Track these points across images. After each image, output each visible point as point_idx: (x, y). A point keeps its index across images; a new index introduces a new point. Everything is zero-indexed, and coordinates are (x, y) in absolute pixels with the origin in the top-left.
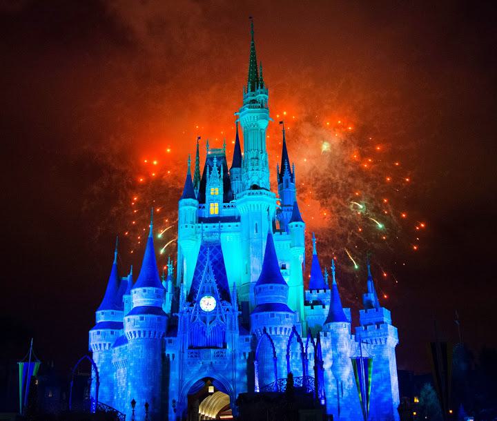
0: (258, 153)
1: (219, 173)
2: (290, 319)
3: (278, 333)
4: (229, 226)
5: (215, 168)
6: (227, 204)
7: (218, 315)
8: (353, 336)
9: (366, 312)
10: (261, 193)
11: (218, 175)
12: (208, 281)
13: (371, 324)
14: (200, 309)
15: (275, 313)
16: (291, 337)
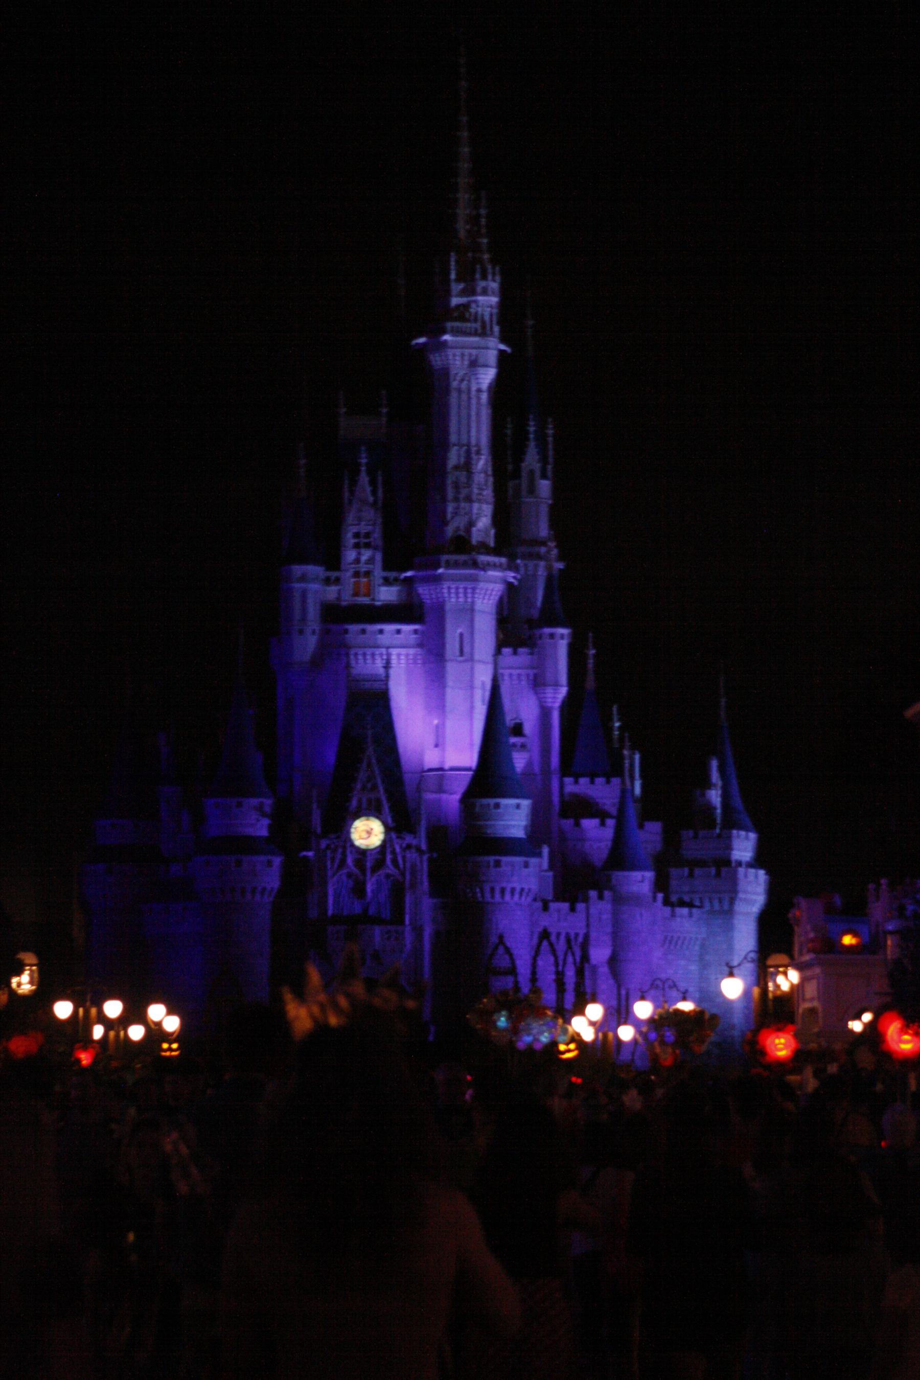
0: (468, 452)
1: (374, 492)
2: (531, 869)
3: (508, 897)
4: (398, 632)
5: (364, 479)
6: (392, 575)
7: (389, 857)
8: (660, 896)
9: (696, 836)
10: (475, 565)
11: (371, 499)
12: (369, 785)
13: (702, 863)
14: (352, 845)
15: (504, 859)
16: (539, 945)
